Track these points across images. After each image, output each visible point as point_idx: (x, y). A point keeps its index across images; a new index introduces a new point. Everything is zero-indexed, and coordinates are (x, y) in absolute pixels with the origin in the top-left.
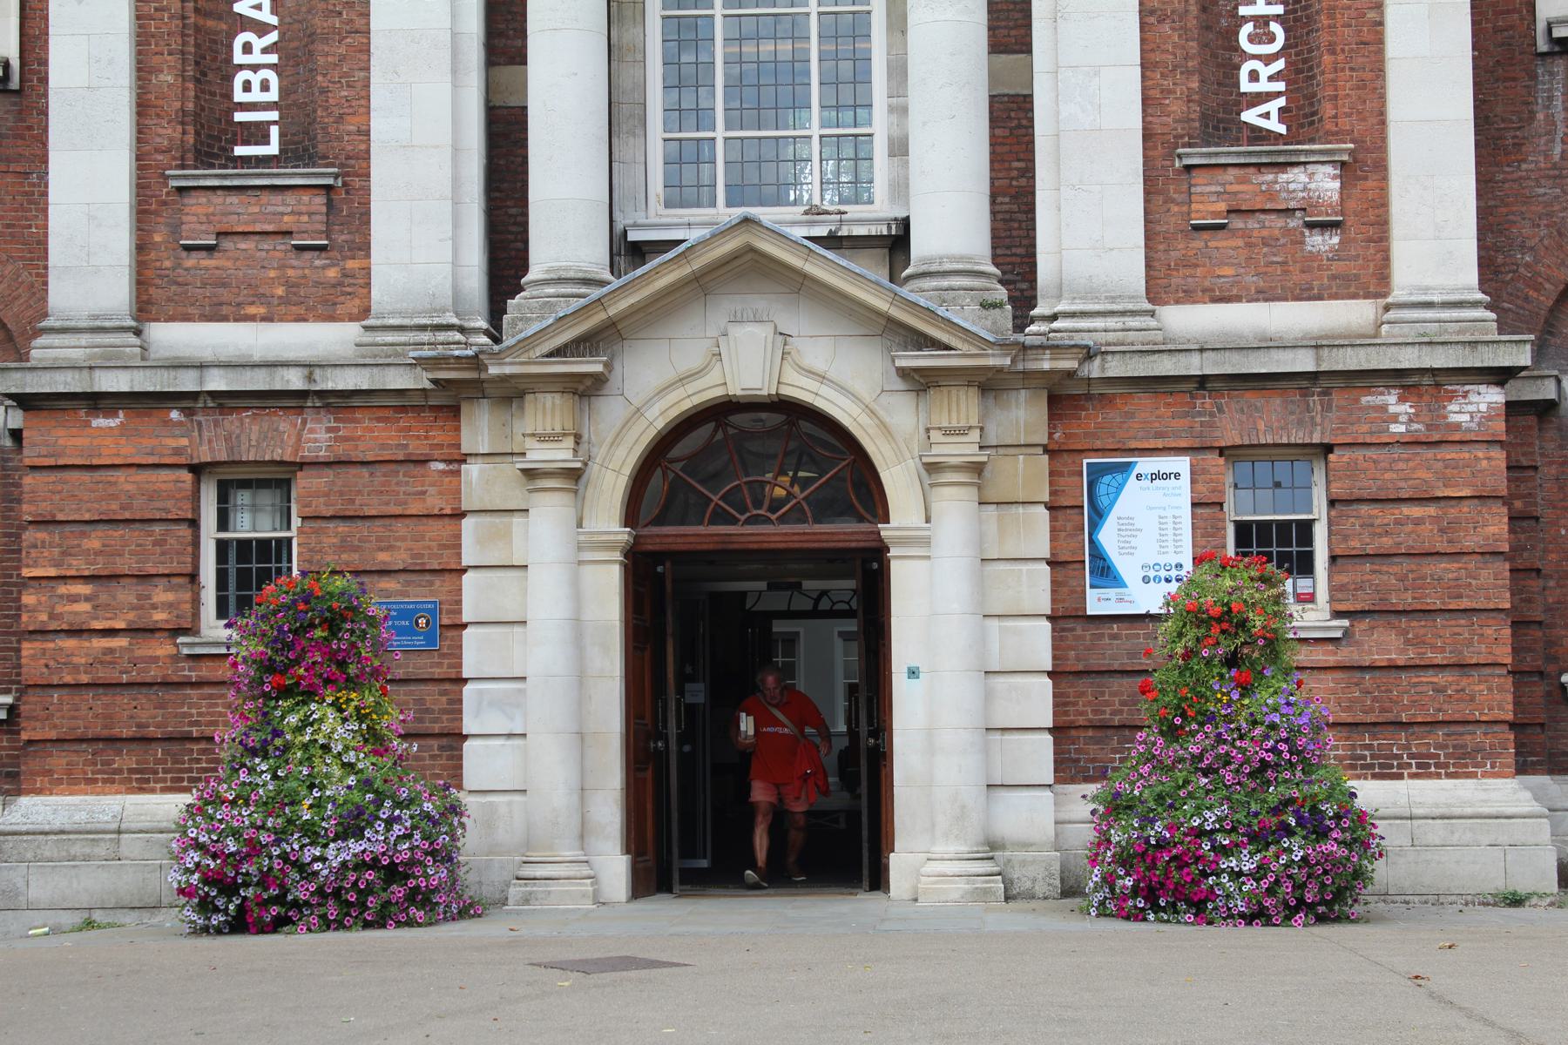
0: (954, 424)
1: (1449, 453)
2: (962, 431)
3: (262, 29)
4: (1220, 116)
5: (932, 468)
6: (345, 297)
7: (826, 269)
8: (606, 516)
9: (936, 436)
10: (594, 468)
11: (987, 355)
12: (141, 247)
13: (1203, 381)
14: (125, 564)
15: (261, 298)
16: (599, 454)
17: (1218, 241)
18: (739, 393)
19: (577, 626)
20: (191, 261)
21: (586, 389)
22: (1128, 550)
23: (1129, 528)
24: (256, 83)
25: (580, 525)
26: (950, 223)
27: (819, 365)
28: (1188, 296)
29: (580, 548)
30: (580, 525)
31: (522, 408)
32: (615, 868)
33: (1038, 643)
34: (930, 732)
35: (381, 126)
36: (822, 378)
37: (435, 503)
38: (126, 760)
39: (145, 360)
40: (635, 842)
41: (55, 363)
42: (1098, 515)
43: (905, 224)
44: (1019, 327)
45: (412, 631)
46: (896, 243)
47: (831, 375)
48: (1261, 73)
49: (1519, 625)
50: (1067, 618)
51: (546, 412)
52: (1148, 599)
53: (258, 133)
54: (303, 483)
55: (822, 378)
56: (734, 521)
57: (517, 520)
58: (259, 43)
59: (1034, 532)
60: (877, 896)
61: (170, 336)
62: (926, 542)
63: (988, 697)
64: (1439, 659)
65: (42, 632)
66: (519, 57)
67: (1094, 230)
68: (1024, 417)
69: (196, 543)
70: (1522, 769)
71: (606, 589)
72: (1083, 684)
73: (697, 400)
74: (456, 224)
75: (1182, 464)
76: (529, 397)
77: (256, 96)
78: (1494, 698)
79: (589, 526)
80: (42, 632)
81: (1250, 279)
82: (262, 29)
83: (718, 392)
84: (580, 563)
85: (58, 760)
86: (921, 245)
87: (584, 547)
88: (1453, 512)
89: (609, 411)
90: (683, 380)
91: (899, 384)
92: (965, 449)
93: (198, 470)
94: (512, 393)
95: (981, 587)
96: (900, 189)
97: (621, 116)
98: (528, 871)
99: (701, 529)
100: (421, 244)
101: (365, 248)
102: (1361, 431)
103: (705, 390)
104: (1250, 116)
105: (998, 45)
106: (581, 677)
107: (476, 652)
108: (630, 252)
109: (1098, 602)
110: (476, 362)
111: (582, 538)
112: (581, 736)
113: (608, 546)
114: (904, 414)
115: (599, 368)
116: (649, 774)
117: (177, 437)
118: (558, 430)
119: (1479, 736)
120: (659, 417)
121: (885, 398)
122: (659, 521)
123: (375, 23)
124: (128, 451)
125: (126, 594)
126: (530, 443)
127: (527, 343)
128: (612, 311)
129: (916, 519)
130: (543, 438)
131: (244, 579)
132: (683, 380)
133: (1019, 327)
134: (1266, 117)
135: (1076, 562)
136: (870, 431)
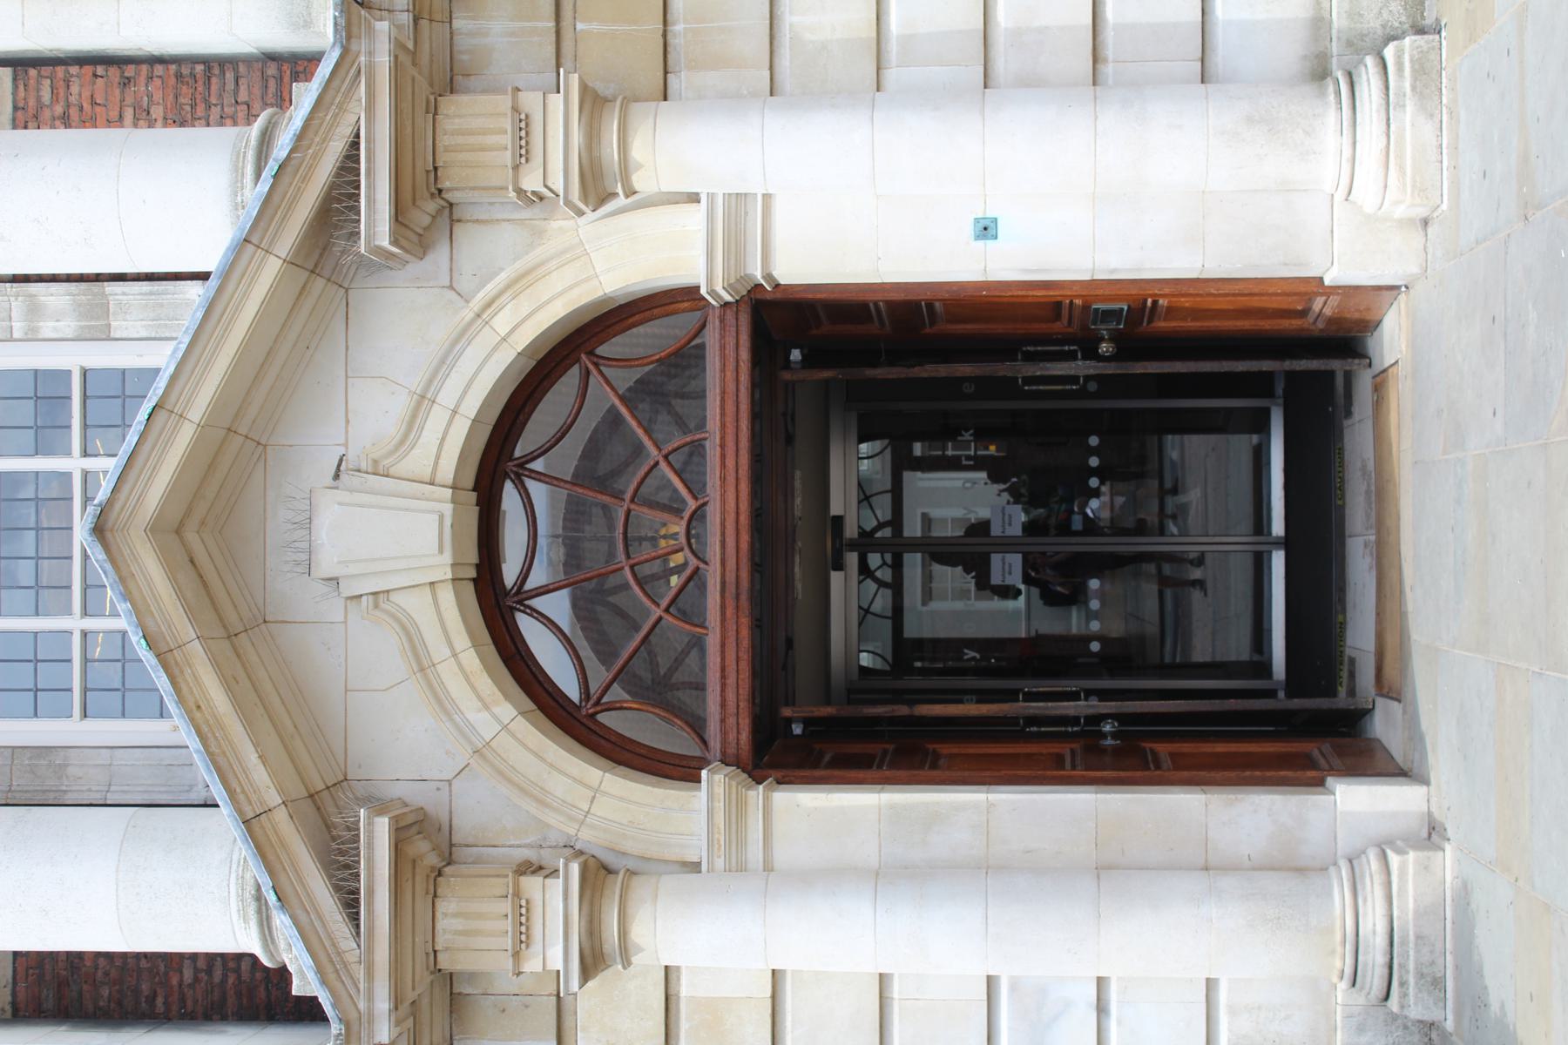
0: (507, 140)
2: (523, 126)
8: (683, 814)
9: (531, 182)
10: (588, 838)
11: (371, 67)
16: (561, 826)
18: (447, 558)
19: (896, 874)
21: (431, 851)
25: (695, 867)
27: (400, 405)
29: (739, 867)
30: (695, 867)
31: (472, 976)
36: (423, 401)
40: (1302, 772)
47: (416, 382)
51: (470, 926)
55: (423, 401)
56: (695, 578)
57: (685, 989)
60: (1393, 340)
62: (738, 200)
63: (1032, 82)
72: (1000, 65)
73: (462, 641)
76: (445, 963)
79: (696, 849)
83: (447, 596)
84: (768, 867)
87: (740, 865)
89: (479, 808)
90: (422, 666)
91: (439, 256)
92: (558, 123)
95: (823, 93)
98: (1374, 978)
99: (713, 641)
106: (989, 871)
111: (720, 863)
112: (1102, 869)
113: (737, 814)
115: (383, 825)
116: (1163, 749)
118: (506, 906)
120: (493, 712)
121: (463, 284)
122: (697, 726)
126: (532, 965)
128: (274, 798)
129: (693, 220)
130: (522, 938)
132: (422, 666)
136: (525, 311)
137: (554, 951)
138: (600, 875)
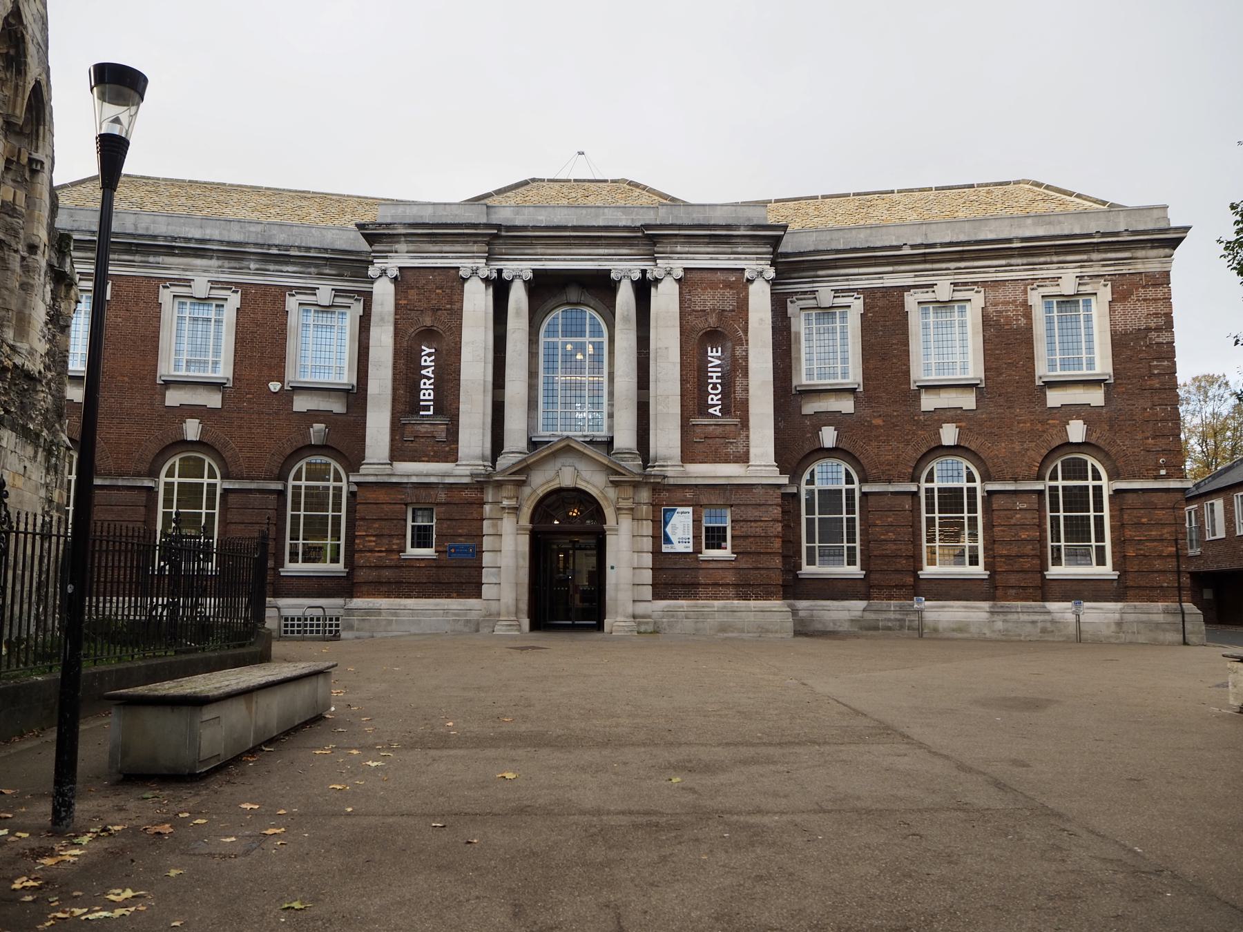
3: (429, 378)
4: (703, 409)
5: (619, 509)
6: (451, 455)
7: (589, 451)
8: (525, 521)
12: (392, 440)
14: (386, 532)
15: (426, 456)
16: (524, 503)
21: (521, 484)
22: (674, 534)
23: (674, 527)
24: (427, 393)
26: (625, 439)
28: (693, 461)
32: (526, 622)
33: (648, 560)
34: (617, 585)
35: (463, 407)
37: (475, 516)
38: (384, 589)
42: (666, 524)
43: (612, 438)
44: (645, 467)
45: (468, 553)
46: (610, 443)
48: (714, 399)
49: (784, 557)
50: (656, 553)
51: (508, 490)
52: (680, 548)
53: (427, 408)
58: (428, 382)
59: (647, 528)
65: (361, 551)
66: (503, 387)
67: (666, 439)
68: (645, 495)
70: (784, 598)
71: (525, 541)
75: (690, 509)
77: (427, 397)
78: (777, 578)
80: (361, 551)
82: (429, 378)
85: (365, 589)
87: (519, 530)
89: (527, 491)
90: (548, 482)
94: (499, 485)
96: (611, 428)
97: (532, 404)
101: (457, 442)
103: (554, 485)
104: (711, 411)
107: (487, 559)
108: (533, 445)
109: (665, 548)
110: (489, 476)
114: (612, 493)
120: (541, 492)
124: (387, 499)
125: (385, 541)
127: (504, 471)
129: (614, 523)
131: (419, 536)
132: (548, 482)
133: (645, 467)
134: (715, 411)
135: (659, 537)
137: (505, 503)
138: (516, 510)
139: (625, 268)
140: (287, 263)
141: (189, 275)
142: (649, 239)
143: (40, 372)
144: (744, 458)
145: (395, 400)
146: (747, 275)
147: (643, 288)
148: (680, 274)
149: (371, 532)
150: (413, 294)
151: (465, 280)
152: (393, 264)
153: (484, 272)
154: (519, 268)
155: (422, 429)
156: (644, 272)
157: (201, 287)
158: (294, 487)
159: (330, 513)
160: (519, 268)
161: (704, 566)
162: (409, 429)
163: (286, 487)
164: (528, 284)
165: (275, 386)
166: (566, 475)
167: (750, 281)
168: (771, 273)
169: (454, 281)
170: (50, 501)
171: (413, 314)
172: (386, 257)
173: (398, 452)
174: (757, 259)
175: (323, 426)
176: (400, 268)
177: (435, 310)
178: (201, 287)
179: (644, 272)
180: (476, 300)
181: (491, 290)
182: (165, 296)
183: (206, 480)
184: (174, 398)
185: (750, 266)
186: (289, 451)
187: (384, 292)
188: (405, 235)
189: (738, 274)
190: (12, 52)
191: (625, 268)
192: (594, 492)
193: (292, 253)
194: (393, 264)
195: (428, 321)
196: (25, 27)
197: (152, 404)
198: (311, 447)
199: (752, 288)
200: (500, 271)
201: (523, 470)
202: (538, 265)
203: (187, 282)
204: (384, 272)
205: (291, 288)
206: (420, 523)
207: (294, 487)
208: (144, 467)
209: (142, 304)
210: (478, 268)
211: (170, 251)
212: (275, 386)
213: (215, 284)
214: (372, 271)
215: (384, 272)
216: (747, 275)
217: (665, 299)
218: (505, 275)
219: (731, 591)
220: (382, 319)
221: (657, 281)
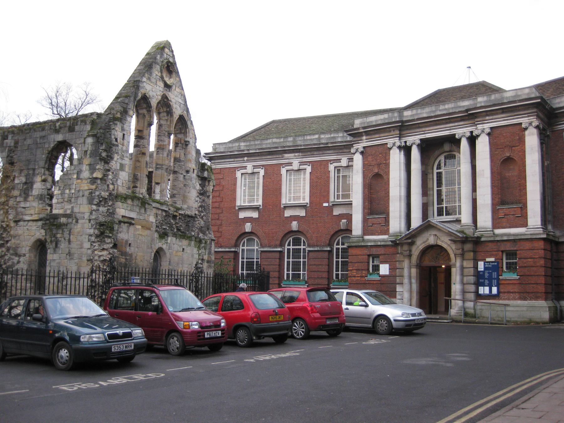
1: (535, 251)
13: (498, 241)
14: (360, 268)
15: (377, 232)
17: (504, 220)
20: (369, 228)
21: (412, 243)
26: (466, 218)
28: (499, 228)
35: (391, 209)
39: (364, 240)
41: (353, 241)
51: (406, 248)
54: (381, 257)
61: (366, 237)
64: (533, 282)
69: (369, 265)
74: (400, 221)
78: (542, 289)
81: (508, 225)
86: (462, 222)
88: (535, 260)
90: (424, 242)
93: (369, 256)
100: (396, 225)
102: (522, 248)
103: (427, 244)
105: (473, 192)
114: (454, 246)
117: (366, 252)
119: (539, 295)
120: (421, 247)
123: (390, 195)
125: (360, 272)
130: (405, 251)
139: (462, 131)
140: (329, 150)
141: (291, 161)
142: (470, 116)
143: (195, 214)
144: (525, 225)
145: (364, 208)
146: (523, 126)
147: (472, 140)
148: (488, 130)
149: (354, 268)
150: (370, 158)
151: (390, 149)
152: (360, 146)
153: (398, 144)
154: (414, 139)
155: (375, 221)
156: (472, 132)
157: (296, 165)
158: (336, 248)
159: (340, 260)
160: (414, 139)
161: (503, 282)
162: (370, 220)
163: (332, 249)
164: (418, 145)
165: (325, 205)
166: (430, 238)
167: (526, 129)
168: (536, 123)
169: (385, 150)
170: (203, 260)
171: (371, 167)
172: (358, 143)
173: (366, 230)
174: (528, 116)
175: (345, 220)
176: (364, 147)
177: (379, 165)
178: (296, 166)
179: (472, 132)
180: (396, 159)
181: (402, 152)
182: (283, 171)
183: (302, 247)
184: (288, 213)
185: (524, 121)
186: (332, 233)
187: (358, 159)
188: (365, 132)
189: (518, 127)
190: (168, 110)
191: (462, 131)
192: (445, 246)
193: (329, 145)
194: (360, 146)
195: (376, 170)
196: (170, 101)
197: (280, 216)
198: (341, 230)
199: (527, 133)
200: (406, 142)
201: (412, 237)
202: (423, 137)
203: (290, 164)
204: (357, 150)
205: (330, 160)
206: (375, 263)
207: (336, 248)
208: (278, 243)
209: (275, 175)
210: (395, 143)
211: (285, 152)
212: (325, 205)
213: (301, 163)
214: (353, 151)
215: (357, 150)
216: (523, 126)
217: (483, 145)
218: (408, 144)
219: (517, 296)
220: (357, 172)
221: (478, 136)
